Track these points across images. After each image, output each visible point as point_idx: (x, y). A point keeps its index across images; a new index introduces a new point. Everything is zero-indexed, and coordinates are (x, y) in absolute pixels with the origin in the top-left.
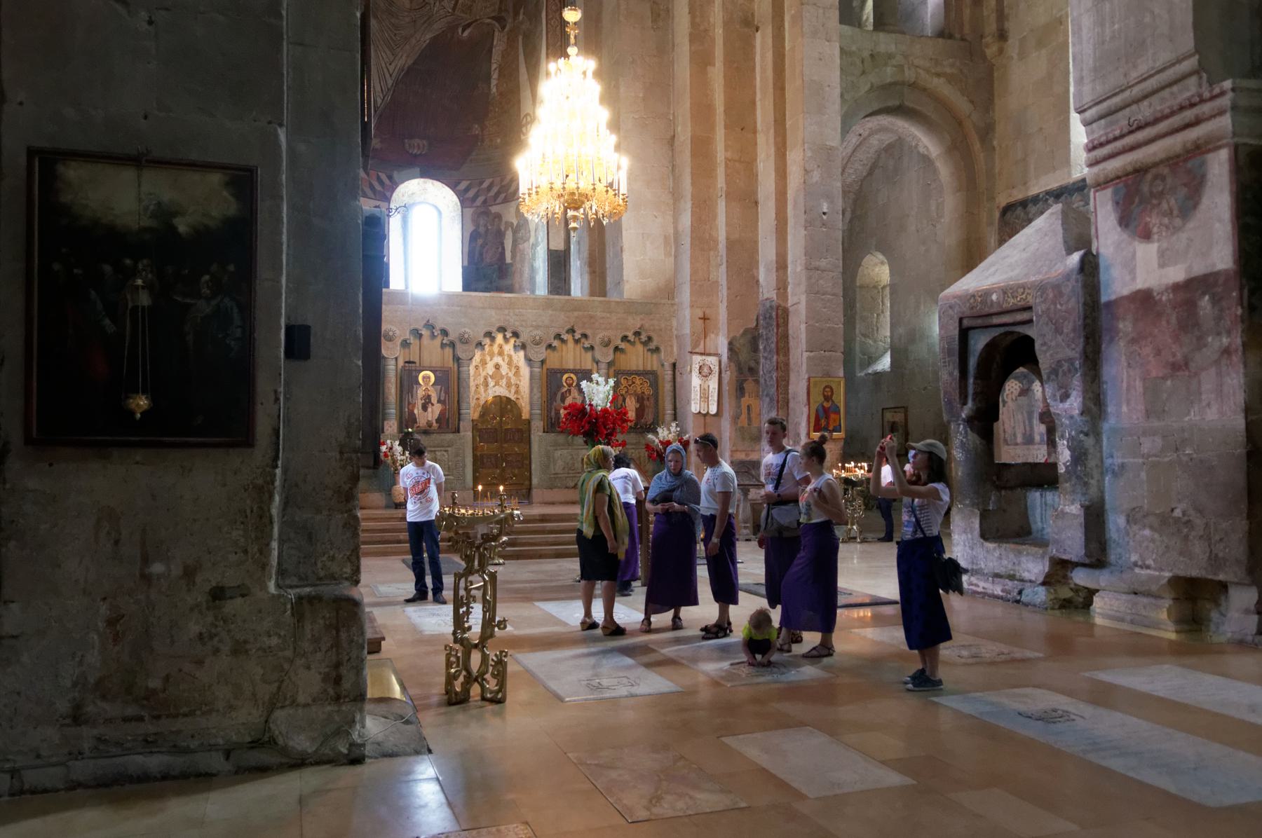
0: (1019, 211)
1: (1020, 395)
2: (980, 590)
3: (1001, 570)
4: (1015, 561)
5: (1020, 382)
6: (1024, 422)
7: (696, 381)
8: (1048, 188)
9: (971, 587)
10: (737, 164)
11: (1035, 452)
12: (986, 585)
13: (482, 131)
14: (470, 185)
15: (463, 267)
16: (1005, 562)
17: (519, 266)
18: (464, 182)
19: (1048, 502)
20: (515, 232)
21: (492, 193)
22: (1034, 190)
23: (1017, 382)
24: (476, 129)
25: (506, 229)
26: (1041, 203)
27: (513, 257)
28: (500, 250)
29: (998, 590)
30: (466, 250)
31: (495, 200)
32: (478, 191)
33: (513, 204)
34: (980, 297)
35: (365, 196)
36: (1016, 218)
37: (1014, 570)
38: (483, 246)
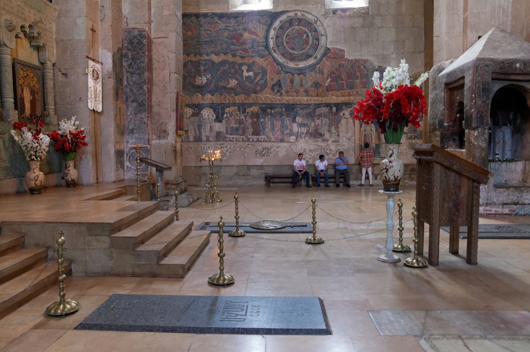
0: (193, 18)
1: (192, 116)
2: (493, 212)
3: (509, 201)
4: (519, 196)
5: (192, 109)
6: (195, 130)
7: (91, 82)
8: (214, 12)
9: (486, 212)
11: (203, 146)
12: (497, 210)
16: (511, 197)
19: (492, 167)
22: (204, 11)
23: (190, 109)
26: (209, 18)
29: (506, 211)
34: (508, 64)
36: (191, 21)
37: (518, 200)
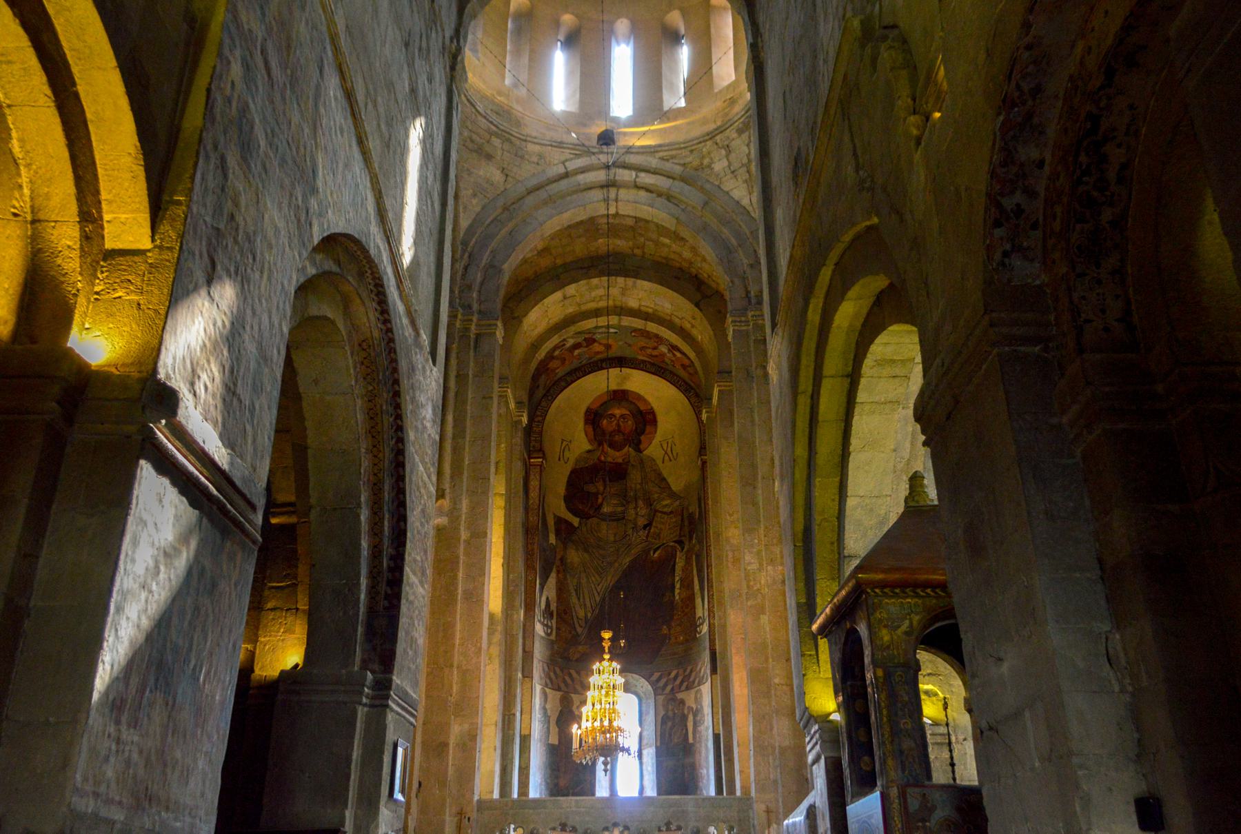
10: (784, 687)
13: (669, 630)
14: (661, 675)
15: (657, 747)
17: (698, 745)
18: (656, 674)
20: (695, 715)
21: (678, 682)
24: (665, 630)
25: (689, 713)
27: (694, 738)
28: (684, 731)
30: (659, 733)
31: (680, 688)
32: (667, 681)
33: (693, 691)
35: (576, 692)
38: (671, 729)
